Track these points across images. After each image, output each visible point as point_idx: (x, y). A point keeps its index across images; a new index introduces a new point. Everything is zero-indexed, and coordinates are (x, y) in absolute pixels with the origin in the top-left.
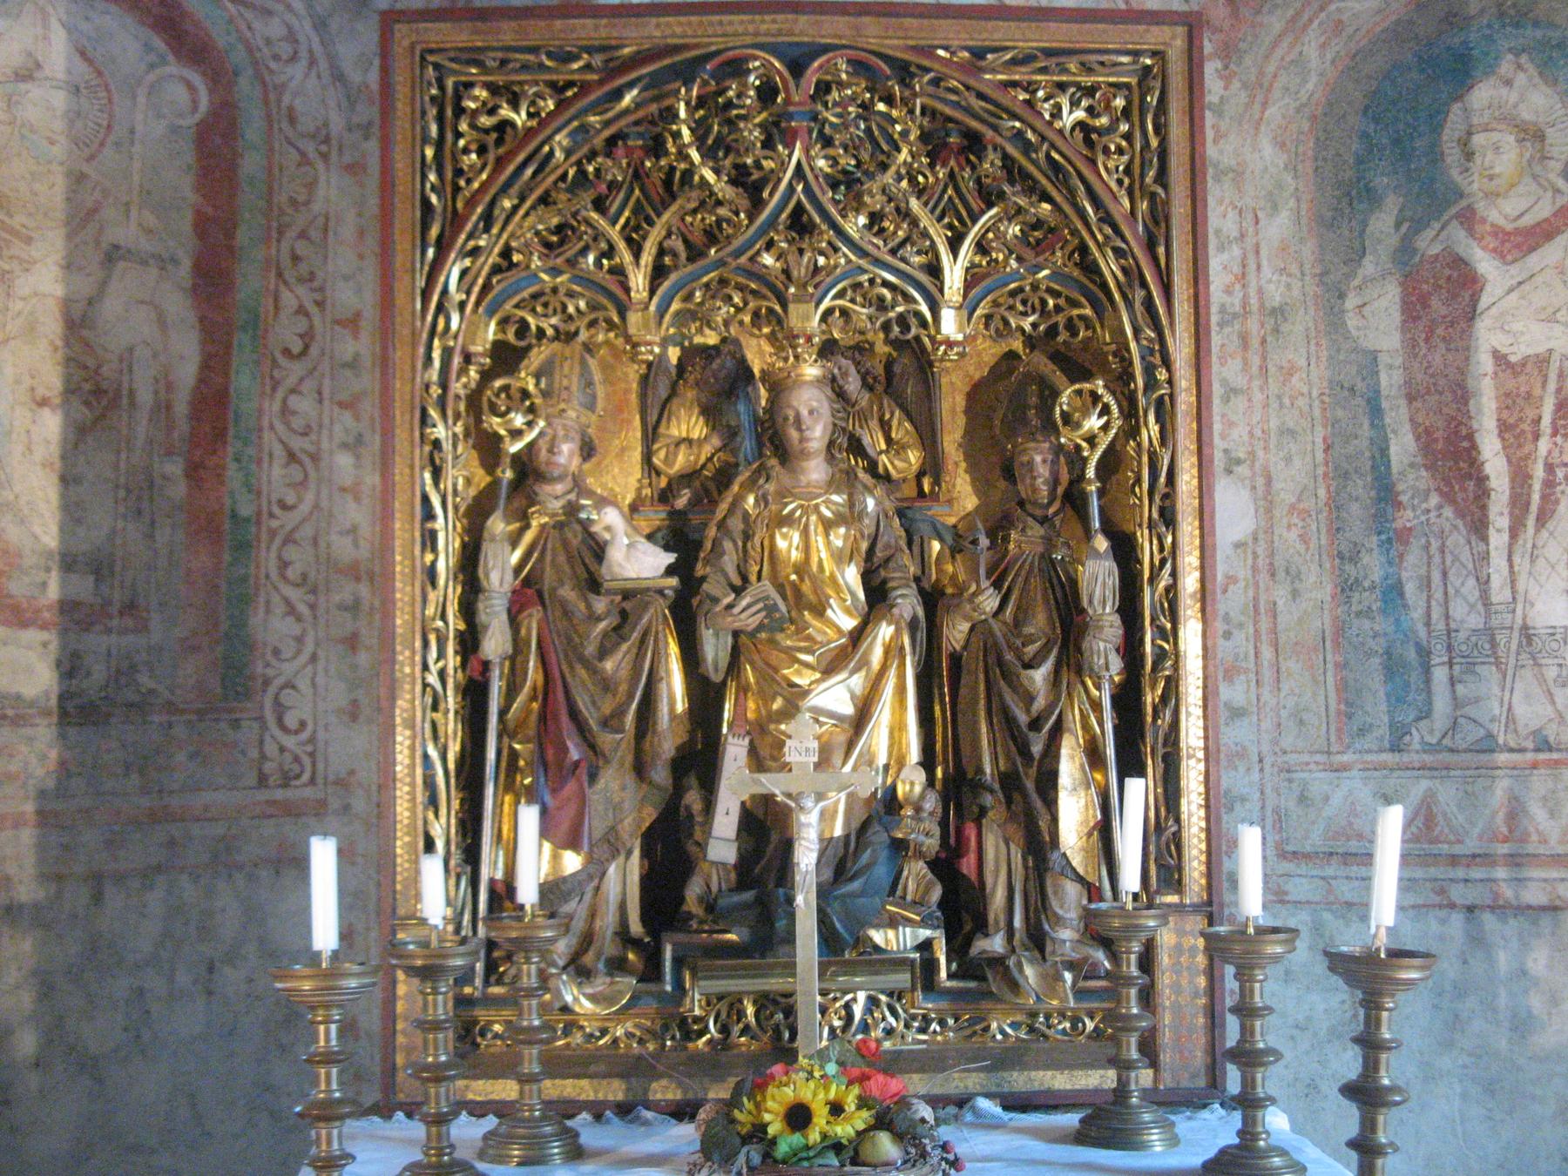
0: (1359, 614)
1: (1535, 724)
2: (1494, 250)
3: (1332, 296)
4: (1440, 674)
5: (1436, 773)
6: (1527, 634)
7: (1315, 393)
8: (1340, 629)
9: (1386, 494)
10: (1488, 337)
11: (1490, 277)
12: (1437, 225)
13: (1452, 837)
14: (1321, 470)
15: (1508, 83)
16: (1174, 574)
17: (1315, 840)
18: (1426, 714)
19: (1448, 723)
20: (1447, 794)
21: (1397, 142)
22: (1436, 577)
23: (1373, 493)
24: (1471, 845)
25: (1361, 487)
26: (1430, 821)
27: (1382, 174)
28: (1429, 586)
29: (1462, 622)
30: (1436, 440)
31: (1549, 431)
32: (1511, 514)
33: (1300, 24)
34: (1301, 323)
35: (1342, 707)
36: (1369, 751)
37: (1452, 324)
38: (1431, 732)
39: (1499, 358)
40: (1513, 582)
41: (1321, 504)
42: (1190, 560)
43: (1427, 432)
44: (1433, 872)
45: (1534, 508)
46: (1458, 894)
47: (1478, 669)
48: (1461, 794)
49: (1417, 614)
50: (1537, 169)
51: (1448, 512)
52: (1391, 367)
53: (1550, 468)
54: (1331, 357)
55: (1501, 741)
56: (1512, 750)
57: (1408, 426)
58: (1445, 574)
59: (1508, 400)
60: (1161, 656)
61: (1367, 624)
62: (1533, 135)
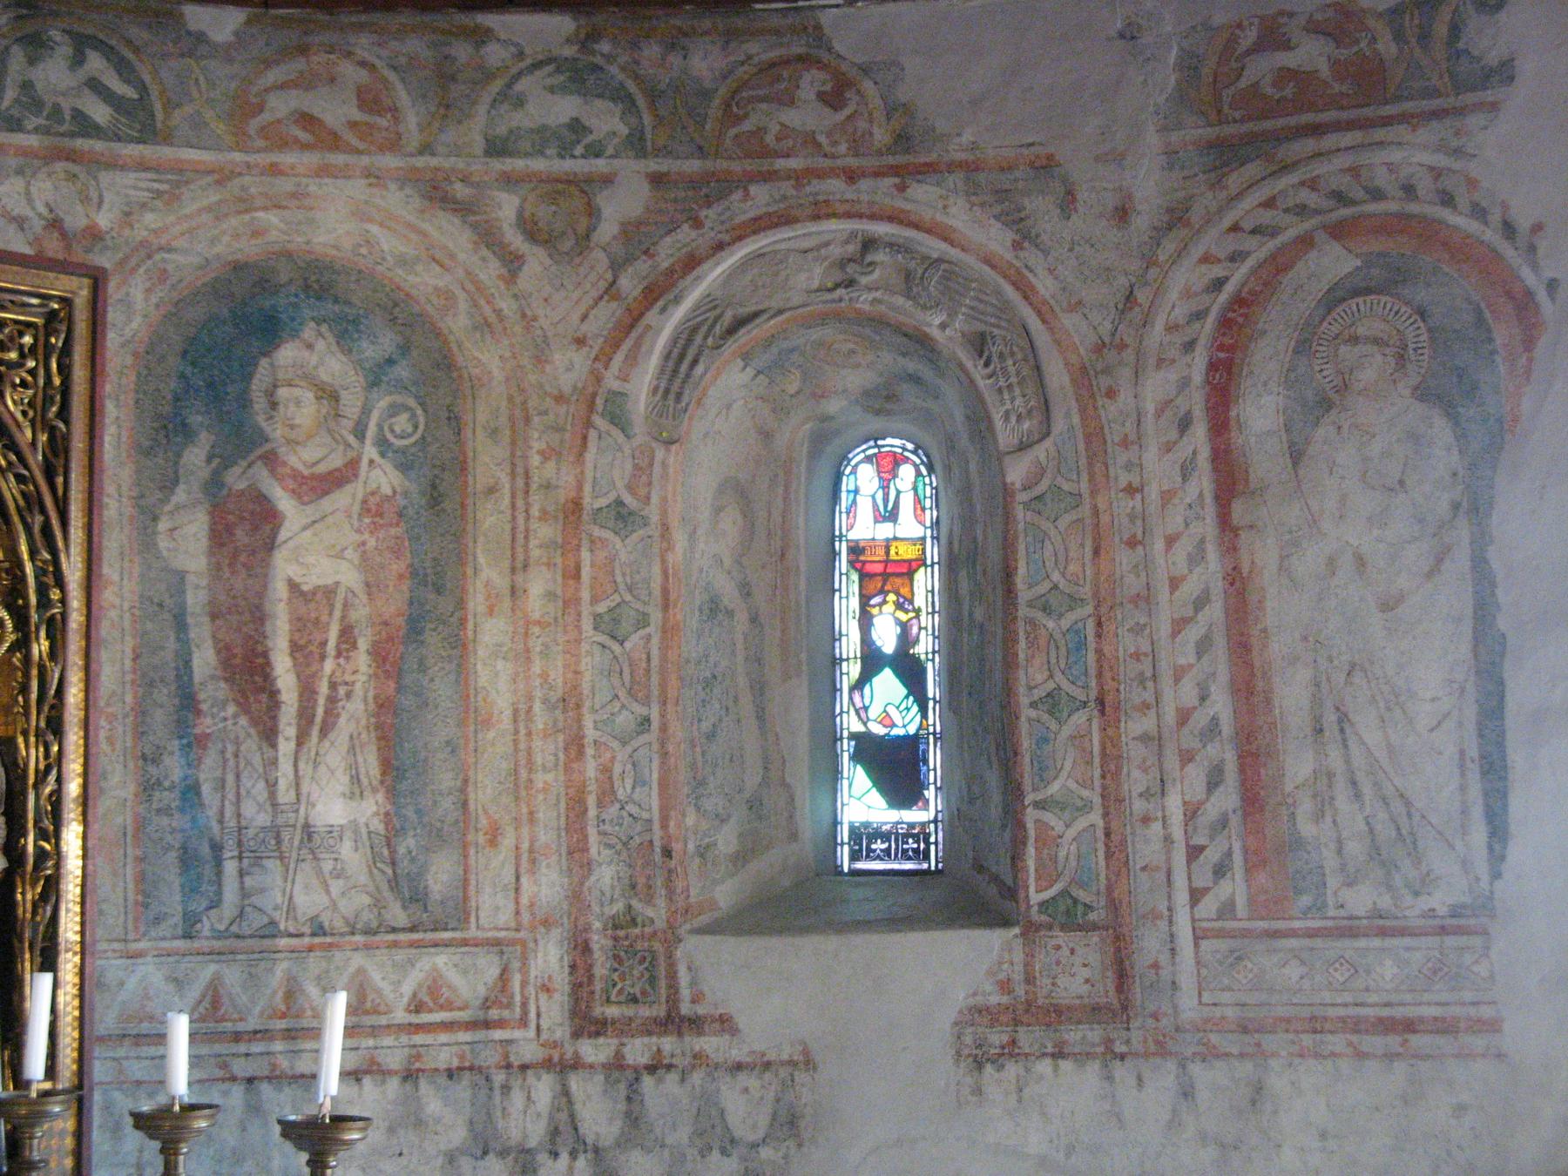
0: (158, 811)
1: (311, 913)
2: (293, 491)
4: (230, 867)
5: (223, 958)
6: (308, 831)
7: (126, 606)
8: (140, 824)
9: (188, 702)
10: (284, 567)
11: (288, 514)
12: (244, 464)
13: (235, 1016)
14: (129, 677)
15: (310, 347)
16: (59, 780)
18: (215, 904)
19: (236, 912)
20: (232, 976)
21: (211, 385)
22: (230, 778)
23: (177, 701)
24: (252, 1024)
25: (164, 695)
26: (216, 1003)
27: (198, 412)
28: (223, 787)
29: (252, 819)
30: (235, 656)
31: (333, 653)
32: (299, 725)
33: (128, 268)
35: (140, 898)
36: (164, 939)
37: (254, 552)
38: (220, 920)
39: (293, 586)
40: (298, 785)
41: (128, 708)
42: (74, 767)
43: (228, 648)
44: (218, 1048)
45: (318, 719)
46: (240, 1068)
47: (265, 862)
48: (245, 976)
49: (212, 812)
50: (332, 424)
51: (243, 721)
52: (197, 587)
53: (333, 686)
54: (142, 575)
55: (282, 927)
56: (291, 935)
57: (210, 642)
58: (238, 776)
59: (300, 624)
60: (41, 855)
61: (165, 821)
62: (329, 395)
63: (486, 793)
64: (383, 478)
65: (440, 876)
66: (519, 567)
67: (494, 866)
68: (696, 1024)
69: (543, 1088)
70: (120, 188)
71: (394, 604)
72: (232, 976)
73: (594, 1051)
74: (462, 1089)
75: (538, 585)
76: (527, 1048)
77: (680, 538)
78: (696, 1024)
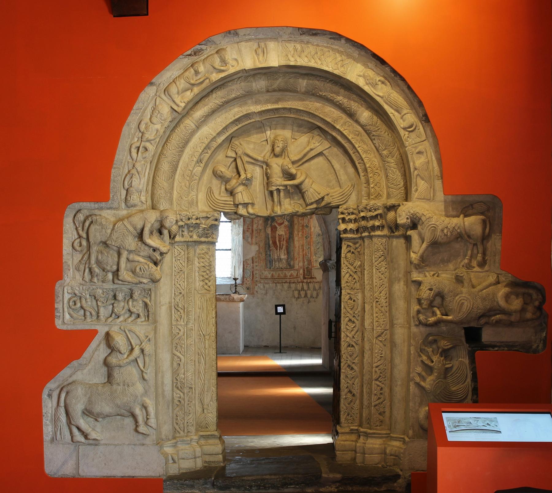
3: (265, 228)
9: (269, 246)
10: (277, 233)
17: (263, 277)
20: (274, 273)
25: (267, 246)
63: (296, 255)
64: (286, 223)
65: (292, 263)
66: (298, 232)
67: (296, 262)
68: (313, 278)
69: (301, 284)
71: (288, 236)
72: (274, 273)
73: (305, 281)
74: (294, 284)
75: (300, 233)
76: (300, 281)
77: (313, 229)
78: (313, 278)
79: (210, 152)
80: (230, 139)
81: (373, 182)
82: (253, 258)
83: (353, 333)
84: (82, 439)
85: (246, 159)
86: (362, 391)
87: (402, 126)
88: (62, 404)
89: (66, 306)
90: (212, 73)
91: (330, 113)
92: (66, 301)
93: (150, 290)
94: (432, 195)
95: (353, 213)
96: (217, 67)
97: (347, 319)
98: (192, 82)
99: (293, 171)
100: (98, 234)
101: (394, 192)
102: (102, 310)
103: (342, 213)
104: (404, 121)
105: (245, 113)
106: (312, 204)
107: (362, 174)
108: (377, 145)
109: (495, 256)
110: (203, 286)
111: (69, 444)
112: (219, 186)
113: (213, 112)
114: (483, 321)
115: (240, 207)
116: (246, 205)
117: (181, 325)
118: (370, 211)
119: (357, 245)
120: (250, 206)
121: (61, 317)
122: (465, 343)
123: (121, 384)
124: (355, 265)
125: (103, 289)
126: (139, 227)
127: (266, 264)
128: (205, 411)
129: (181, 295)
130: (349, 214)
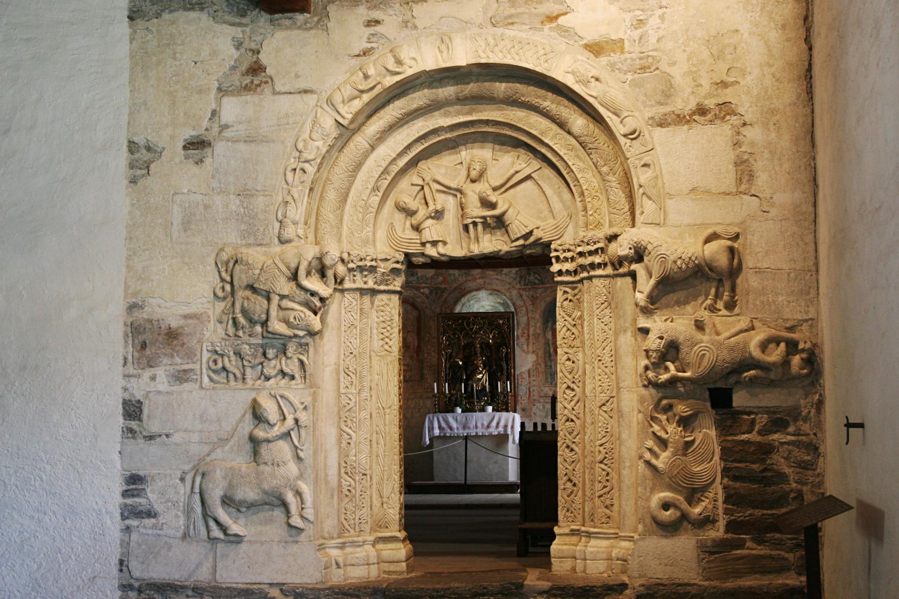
3: (544, 332)
34: (541, 335)
70: (539, 291)
79: (389, 178)
80: (414, 163)
81: (592, 209)
82: (529, 371)
83: (573, 403)
84: (222, 536)
85: (436, 186)
86: (584, 480)
87: (622, 132)
88: (197, 490)
89: (204, 366)
90: (385, 77)
91: (535, 124)
92: (204, 360)
93: (307, 344)
94: (662, 218)
95: (569, 250)
96: (391, 68)
97: (565, 386)
98: (361, 88)
99: (493, 198)
100: (243, 276)
101: (618, 218)
102: (249, 371)
103: (556, 250)
104: (624, 126)
105: (432, 128)
106: (517, 239)
107: (578, 199)
108: (595, 161)
109: (748, 294)
110: (382, 346)
111: (205, 541)
112: (403, 221)
113: (392, 128)
114: (732, 379)
115: (428, 245)
116: (434, 243)
117: (352, 393)
118: (588, 244)
119: (576, 291)
120: (440, 244)
121: (199, 380)
122: (710, 409)
123: (269, 463)
124: (573, 316)
125: (249, 345)
126: (293, 265)
127: (546, 378)
128: (385, 505)
129: (352, 356)
130: (564, 251)
